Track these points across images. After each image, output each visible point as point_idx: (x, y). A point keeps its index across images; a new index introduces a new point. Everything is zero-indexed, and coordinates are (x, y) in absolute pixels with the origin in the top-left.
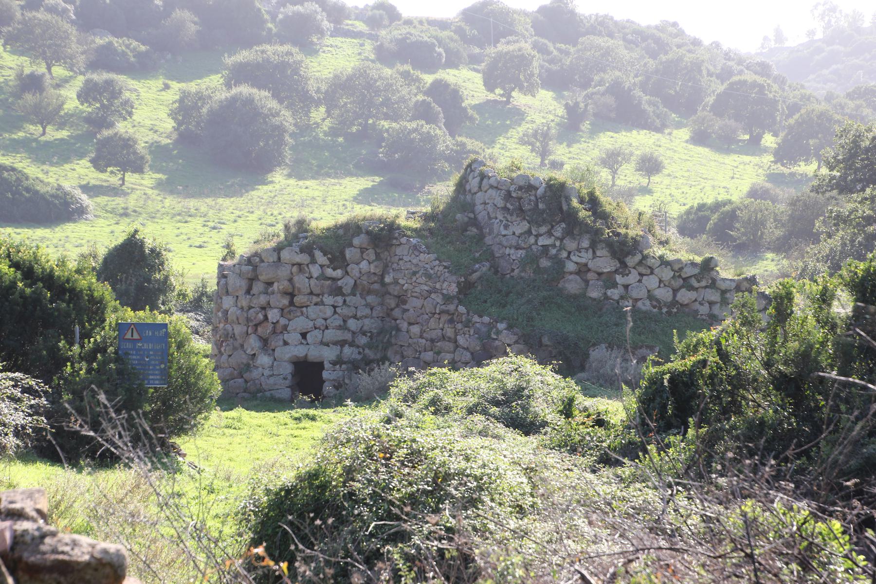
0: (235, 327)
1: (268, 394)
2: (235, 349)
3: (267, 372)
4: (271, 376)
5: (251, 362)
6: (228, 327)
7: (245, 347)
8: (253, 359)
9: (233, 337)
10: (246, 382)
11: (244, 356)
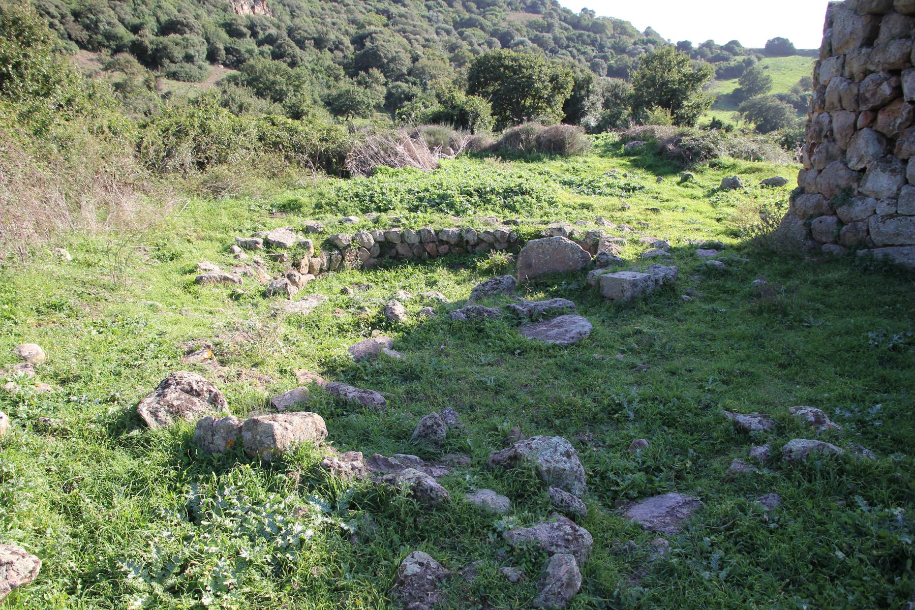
0: (834, 115)
1: (878, 253)
2: (830, 158)
3: (883, 208)
4: (891, 216)
5: (855, 186)
6: (825, 118)
7: (848, 155)
8: (858, 180)
9: (830, 136)
10: (841, 223)
11: (842, 172)
